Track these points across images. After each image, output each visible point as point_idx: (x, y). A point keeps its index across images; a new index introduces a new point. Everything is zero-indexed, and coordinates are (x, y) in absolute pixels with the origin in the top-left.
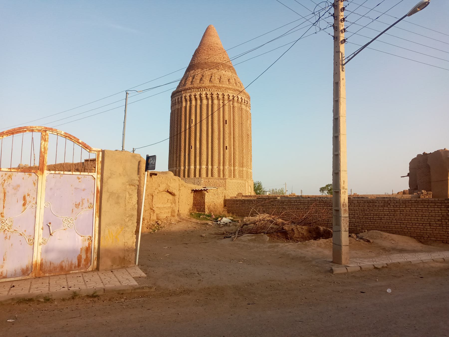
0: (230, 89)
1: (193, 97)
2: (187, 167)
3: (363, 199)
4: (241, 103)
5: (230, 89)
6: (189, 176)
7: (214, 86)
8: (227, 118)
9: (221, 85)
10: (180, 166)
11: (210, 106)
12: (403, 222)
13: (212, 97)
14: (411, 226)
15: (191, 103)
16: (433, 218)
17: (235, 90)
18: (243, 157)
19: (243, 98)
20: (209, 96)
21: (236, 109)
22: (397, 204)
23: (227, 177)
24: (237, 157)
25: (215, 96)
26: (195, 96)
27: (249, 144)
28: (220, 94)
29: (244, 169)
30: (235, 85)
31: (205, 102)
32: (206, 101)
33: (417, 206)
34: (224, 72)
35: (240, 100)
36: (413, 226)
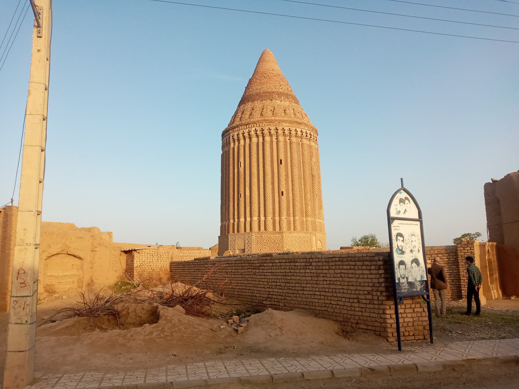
0: (285, 121)
1: (241, 136)
2: (236, 220)
3: (286, 257)
4: (301, 137)
5: (285, 121)
6: (238, 231)
8: (282, 157)
9: (273, 118)
10: (229, 220)
12: (328, 294)
13: (262, 133)
14: (335, 303)
15: (239, 143)
16: (362, 288)
17: (292, 122)
18: (306, 204)
19: (304, 131)
20: (259, 133)
21: (294, 146)
22: (320, 264)
24: (298, 204)
25: (266, 132)
26: (243, 134)
27: (316, 187)
28: (273, 128)
29: (309, 219)
30: (293, 116)
31: (254, 140)
32: (256, 139)
33: (341, 267)
34: (279, 102)
35: (299, 133)
36: (339, 303)
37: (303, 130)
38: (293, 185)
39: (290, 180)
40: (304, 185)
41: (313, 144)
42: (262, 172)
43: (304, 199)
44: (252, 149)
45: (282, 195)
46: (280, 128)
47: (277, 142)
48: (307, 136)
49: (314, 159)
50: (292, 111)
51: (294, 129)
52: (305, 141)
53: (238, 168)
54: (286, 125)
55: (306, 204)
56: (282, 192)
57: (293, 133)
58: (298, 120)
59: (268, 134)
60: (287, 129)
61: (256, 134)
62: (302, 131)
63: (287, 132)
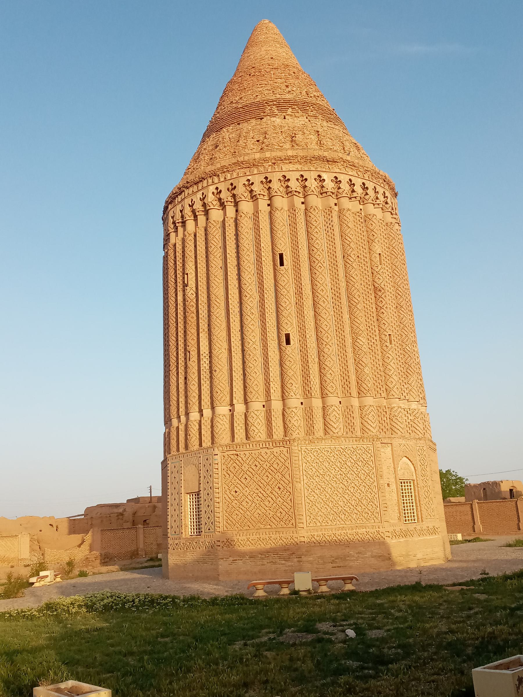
0: (289, 160)
5: (289, 160)
7: (237, 164)
9: (257, 156)
13: (234, 196)
17: (309, 160)
20: (225, 195)
21: (318, 219)
23: (295, 435)
25: (241, 190)
28: (257, 179)
30: (314, 146)
31: (216, 214)
32: (221, 212)
35: (329, 185)
37: (341, 177)
38: (316, 314)
39: (308, 303)
40: (351, 313)
41: (371, 209)
42: (237, 291)
43: (350, 350)
44: (210, 237)
45: (288, 342)
46: (275, 177)
48: (353, 191)
49: (378, 249)
50: (314, 137)
51: (314, 175)
52: (345, 203)
54: (291, 167)
55: (358, 363)
56: (288, 337)
57: (312, 184)
58: (326, 154)
59: (247, 194)
60: (293, 176)
61: (220, 199)
63: (294, 185)
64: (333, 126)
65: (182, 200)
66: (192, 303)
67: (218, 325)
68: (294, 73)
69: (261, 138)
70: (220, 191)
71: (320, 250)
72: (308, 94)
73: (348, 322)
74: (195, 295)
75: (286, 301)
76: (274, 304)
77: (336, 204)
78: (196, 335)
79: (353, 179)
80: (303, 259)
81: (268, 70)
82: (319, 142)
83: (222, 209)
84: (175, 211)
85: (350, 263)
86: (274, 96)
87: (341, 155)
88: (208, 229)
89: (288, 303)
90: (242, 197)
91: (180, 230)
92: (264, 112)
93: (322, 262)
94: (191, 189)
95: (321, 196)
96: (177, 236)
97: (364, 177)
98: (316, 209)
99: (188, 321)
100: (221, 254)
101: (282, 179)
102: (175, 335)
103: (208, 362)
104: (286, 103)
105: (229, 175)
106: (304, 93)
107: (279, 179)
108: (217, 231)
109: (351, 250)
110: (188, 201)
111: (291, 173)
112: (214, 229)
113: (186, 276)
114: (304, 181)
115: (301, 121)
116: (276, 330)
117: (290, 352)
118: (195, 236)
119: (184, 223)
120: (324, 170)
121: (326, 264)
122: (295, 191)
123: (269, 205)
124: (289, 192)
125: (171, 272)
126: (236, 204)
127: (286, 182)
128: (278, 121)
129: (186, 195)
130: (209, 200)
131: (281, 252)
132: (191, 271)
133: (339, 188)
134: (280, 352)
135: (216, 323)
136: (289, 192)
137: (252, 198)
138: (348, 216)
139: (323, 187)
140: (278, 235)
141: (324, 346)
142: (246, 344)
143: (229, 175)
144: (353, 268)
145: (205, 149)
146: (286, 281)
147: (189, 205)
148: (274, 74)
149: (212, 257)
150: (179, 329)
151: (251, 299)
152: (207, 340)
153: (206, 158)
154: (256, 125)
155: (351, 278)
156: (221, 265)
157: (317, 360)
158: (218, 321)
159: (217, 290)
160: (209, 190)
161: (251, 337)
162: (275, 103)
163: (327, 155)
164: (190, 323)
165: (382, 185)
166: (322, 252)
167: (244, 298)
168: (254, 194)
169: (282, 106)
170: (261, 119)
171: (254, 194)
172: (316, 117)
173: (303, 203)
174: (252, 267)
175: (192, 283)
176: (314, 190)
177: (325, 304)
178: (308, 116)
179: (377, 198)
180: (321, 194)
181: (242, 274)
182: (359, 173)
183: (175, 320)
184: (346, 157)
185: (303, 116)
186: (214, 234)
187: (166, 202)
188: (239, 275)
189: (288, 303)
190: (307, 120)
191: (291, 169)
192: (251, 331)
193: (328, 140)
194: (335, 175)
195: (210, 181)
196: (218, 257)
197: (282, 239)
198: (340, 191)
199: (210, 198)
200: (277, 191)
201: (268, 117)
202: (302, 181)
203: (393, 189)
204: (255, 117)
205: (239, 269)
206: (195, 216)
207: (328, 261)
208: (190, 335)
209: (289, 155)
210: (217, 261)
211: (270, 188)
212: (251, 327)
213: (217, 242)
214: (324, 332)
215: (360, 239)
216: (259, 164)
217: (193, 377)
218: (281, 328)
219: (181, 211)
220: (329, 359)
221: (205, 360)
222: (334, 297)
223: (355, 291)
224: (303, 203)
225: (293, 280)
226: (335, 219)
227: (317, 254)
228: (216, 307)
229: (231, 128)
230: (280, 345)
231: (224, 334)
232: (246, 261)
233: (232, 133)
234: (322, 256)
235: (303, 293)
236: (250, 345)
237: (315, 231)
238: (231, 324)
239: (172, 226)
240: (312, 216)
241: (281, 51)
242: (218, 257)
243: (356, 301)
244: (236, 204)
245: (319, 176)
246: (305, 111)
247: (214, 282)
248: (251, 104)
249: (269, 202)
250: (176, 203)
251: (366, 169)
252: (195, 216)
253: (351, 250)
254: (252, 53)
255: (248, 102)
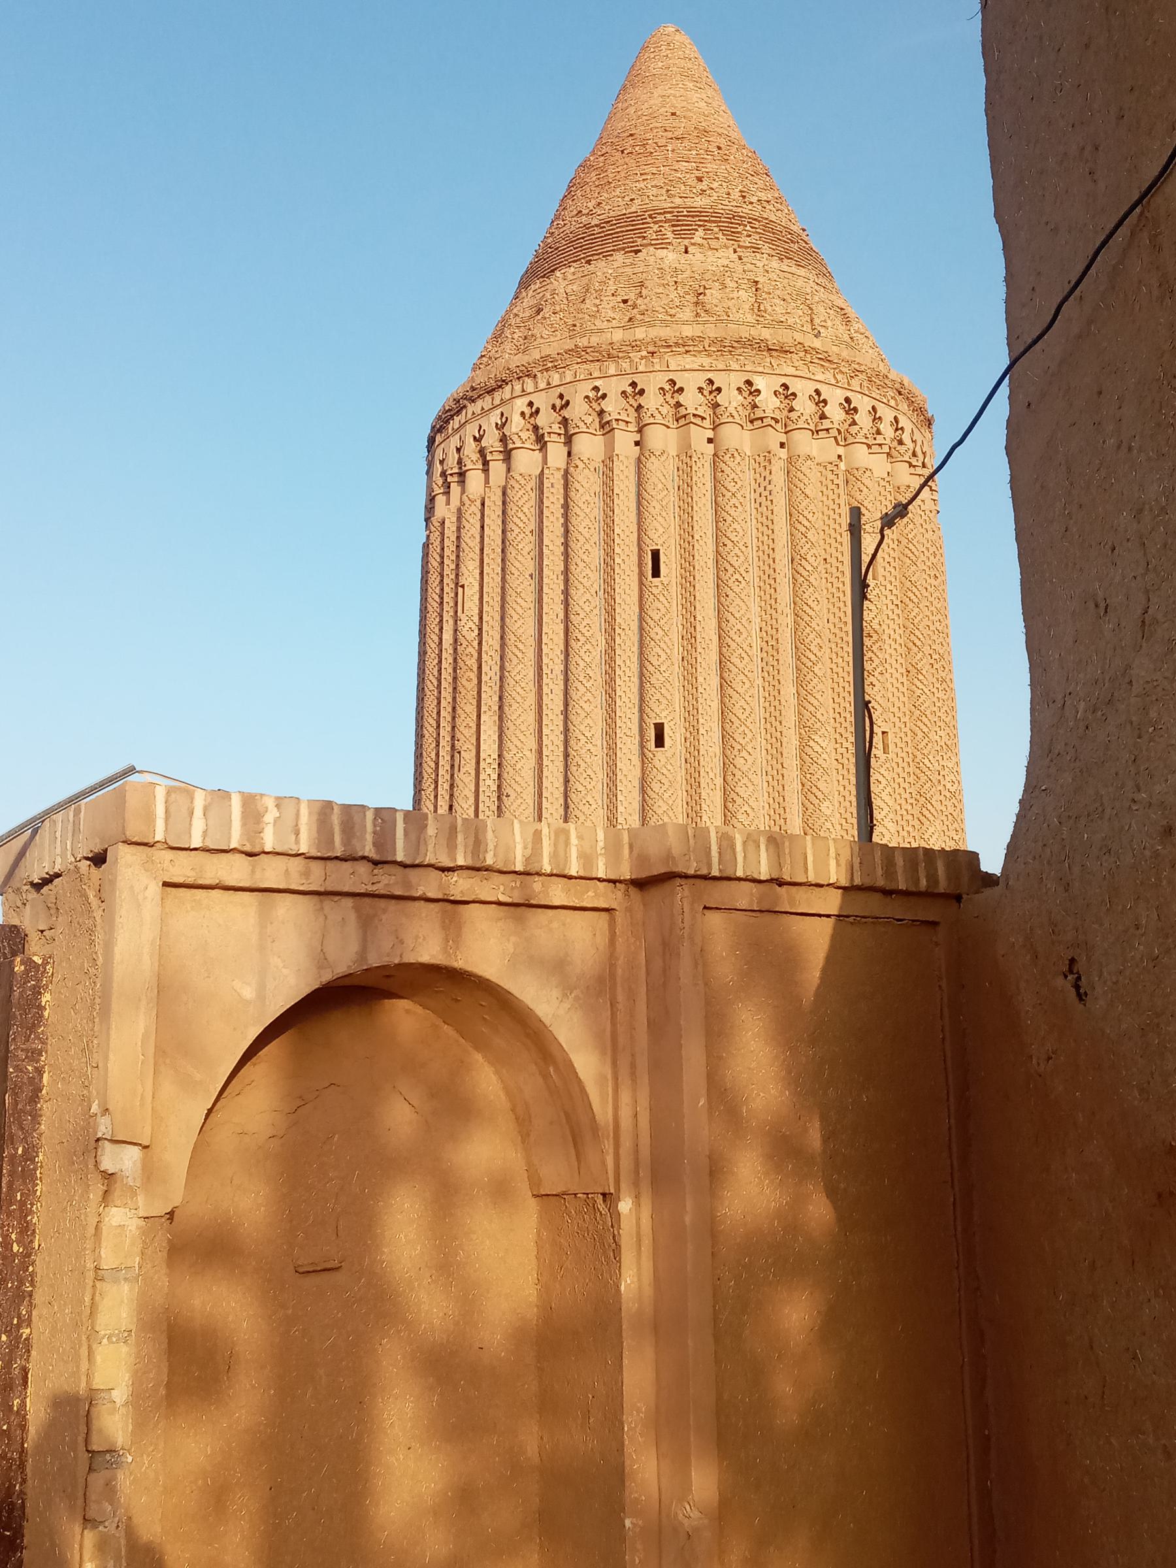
0: (684, 346)
5: (684, 346)
7: (575, 351)
9: (618, 336)
11: (554, 481)
13: (565, 422)
17: (726, 347)
20: (546, 420)
21: (741, 476)
25: (579, 410)
31: (526, 460)
32: (538, 455)
35: (769, 403)
37: (796, 386)
39: (708, 658)
44: (512, 509)
45: (660, 742)
46: (653, 383)
47: (639, 460)
48: (823, 417)
51: (738, 380)
53: (456, 620)
54: (689, 361)
56: (659, 729)
57: (731, 400)
58: (766, 334)
59: (592, 419)
60: (691, 382)
61: (536, 428)
62: (787, 393)
63: (692, 401)
64: (794, 269)
65: (462, 426)
66: (470, 649)
67: (519, 699)
68: (719, 148)
69: (632, 297)
70: (538, 411)
71: (740, 545)
72: (744, 197)
73: (793, 701)
74: (476, 632)
75: (661, 652)
76: (635, 659)
77: (782, 445)
78: (475, 718)
79: (823, 389)
80: (702, 563)
81: (662, 142)
82: (756, 305)
83: (540, 450)
84: (448, 448)
85: (805, 573)
86: (669, 200)
87: (799, 337)
88: (509, 491)
89: (664, 656)
90: (581, 424)
91: (455, 489)
92: (644, 238)
93: (742, 570)
94: (479, 403)
95: (750, 426)
96: (448, 503)
97: (849, 384)
98: (736, 454)
99: (460, 688)
100: (531, 546)
101: (667, 387)
102: (435, 716)
103: (495, 776)
104: (693, 216)
105: (557, 376)
106: (736, 194)
107: (662, 389)
108: (526, 498)
109: (808, 546)
110: (472, 430)
111: (686, 374)
112: (521, 493)
113: (460, 590)
114: (715, 394)
115: (723, 257)
116: (637, 714)
117: (663, 763)
118: (483, 504)
119: (462, 475)
120: (761, 369)
121: (753, 575)
122: (694, 415)
123: (637, 443)
124: (681, 418)
125: (434, 578)
126: (569, 440)
127: (676, 395)
128: (670, 257)
129: (469, 416)
130: (514, 430)
131: (655, 547)
132: (471, 579)
133: (792, 410)
134: (643, 762)
135: (514, 694)
136: (681, 418)
137: (602, 427)
138: (807, 472)
139: (755, 406)
140: (651, 509)
141: (736, 752)
142: (572, 743)
143: (557, 376)
144: (811, 585)
145: (516, 315)
146: (663, 610)
147: (475, 438)
148: (673, 151)
149: (514, 552)
150: (443, 703)
151: (588, 646)
152: (496, 728)
153: (516, 336)
154: (625, 265)
155: (805, 608)
156: (531, 570)
157: (719, 781)
158: (519, 689)
159: (519, 623)
160: (515, 408)
161: (582, 728)
162: (668, 216)
163: (768, 337)
164: (463, 692)
165: (892, 403)
166: (744, 549)
167: (572, 643)
168: (607, 418)
169: (685, 222)
170: (637, 252)
171: (607, 418)
172: (756, 249)
173: (710, 441)
174: (594, 576)
175: (472, 606)
176: (735, 414)
177: (744, 662)
178: (739, 246)
179: (878, 432)
180: (752, 422)
181: (572, 592)
182: (839, 377)
183: (436, 684)
184: (811, 342)
185: (727, 248)
186: (520, 504)
187: (433, 427)
188: (566, 593)
189: (664, 656)
190: (735, 256)
191: (688, 367)
192: (583, 714)
193: (777, 301)
194: (784, 380)
195: (518, 387)
196: (525, 553)
197: (659, 518)
198: (793, 415)
199: (516, 424)
200: (656, 414)
201: (651, 248)
202: (711, 392)
203: (920, 411)
204: (623, 249)
205: (567, 581)
206: (486, 463)
207: (756, 569)
208: (463, 716)
209: (684, 334)
210: (522, 563)
211: (640, 407)
212: (585, 706)
213: (525, 520)
214: (737, 722)
215: (831, 522)
216: (621, 355)
217: (465, 806)
218: (647, 710)
219: (458, 450)
220: (745, 780)
221: (489, 771)
222: (765, 648)
223: (812, 636)
224: (710, 441)
225: (680, 607)
226: (779, 478)
227: (732, 554)
228: (515, 661)
229: (572, 269)
230: (642, 746)
231: (531, 717)
232: (582, 565)
233: (572, 282)
234: (742, 558)
235: (698, 637)
236: (580, 744)
237: (731, 504)
238: (545, 697)
239: (440, 481)
240: (727, 470)
241: (695, 96)
242: (525, 553)
243: (813, 657)
244: (569, 440)
245: (749, 383)
246: (733, 235)
247: (515, 606)
248: (619, 218)
249: (637, 437)
250: (450, 431)
251: (856, 366)
252: (486, 463)
253: (808, 546)
254: (632, 102)
255: (612, 214)
